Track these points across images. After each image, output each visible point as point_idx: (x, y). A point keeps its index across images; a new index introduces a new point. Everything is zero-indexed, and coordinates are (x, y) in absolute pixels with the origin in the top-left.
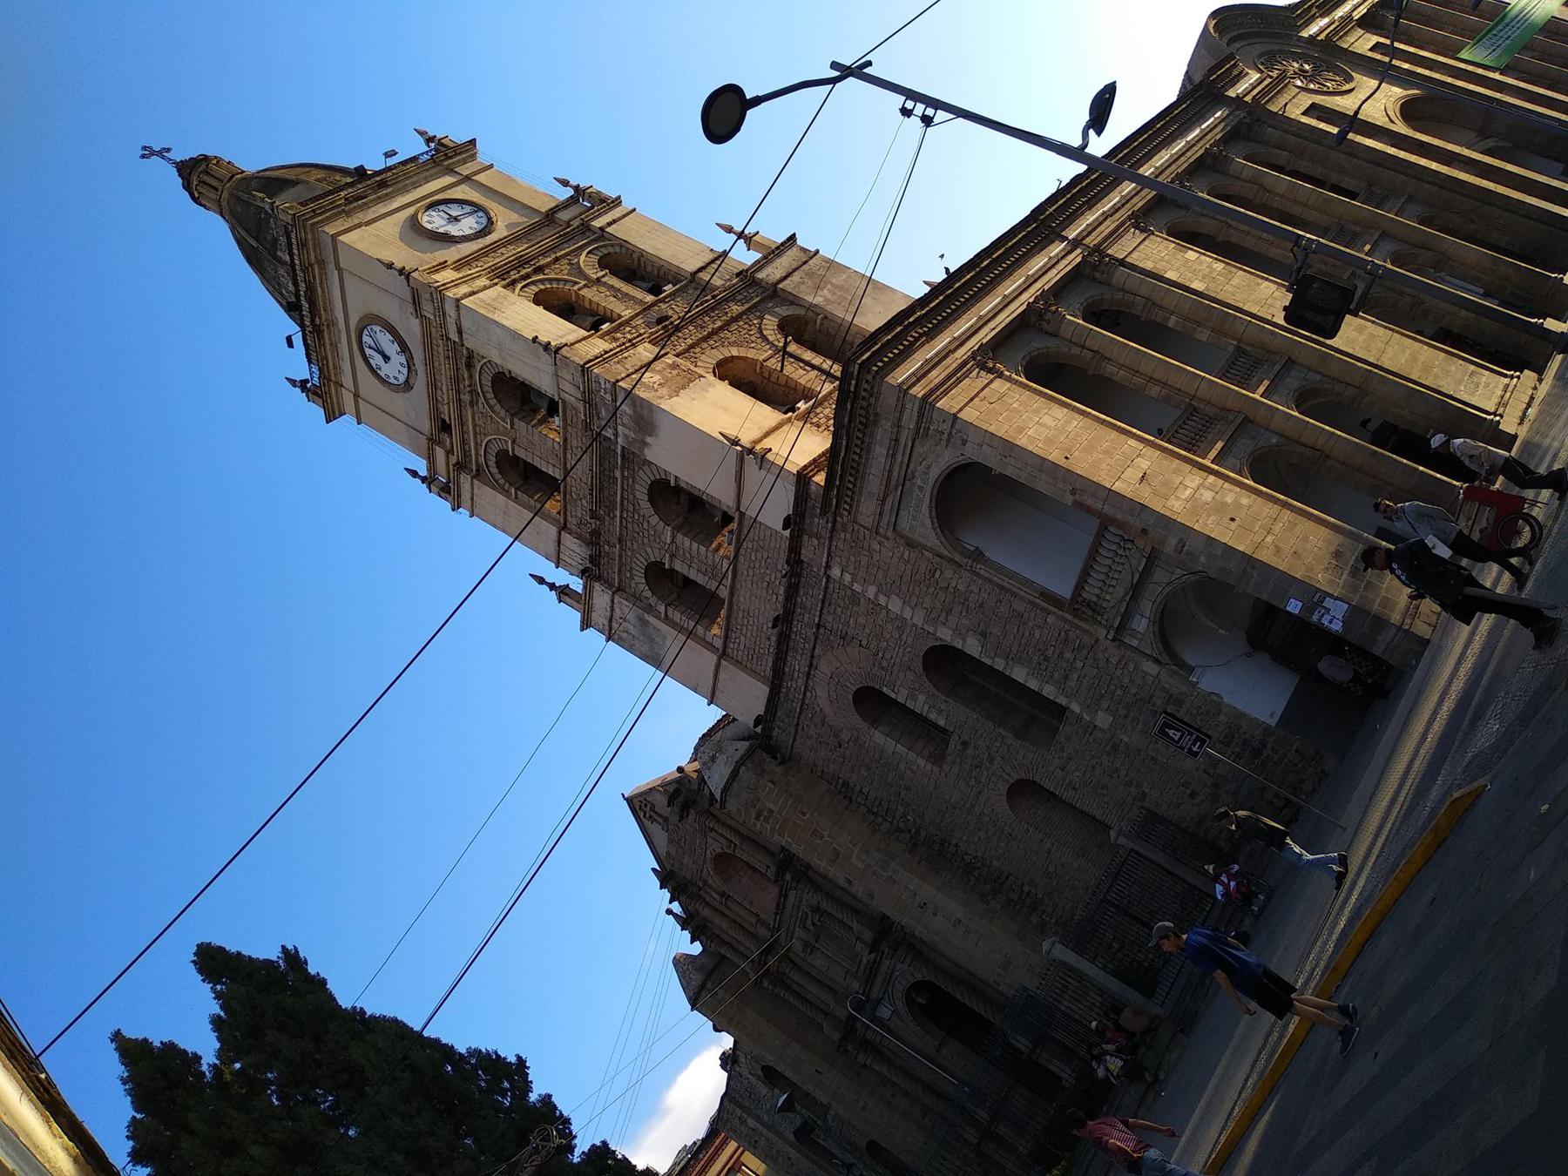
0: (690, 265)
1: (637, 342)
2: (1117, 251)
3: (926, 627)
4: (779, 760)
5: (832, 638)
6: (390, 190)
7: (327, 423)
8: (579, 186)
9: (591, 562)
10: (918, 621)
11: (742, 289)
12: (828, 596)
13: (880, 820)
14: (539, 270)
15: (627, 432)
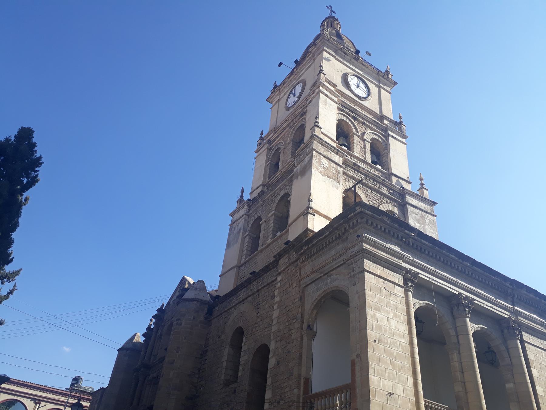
0: (394, 171)
1: (339, 154)
2: (526, 337)
3: (272, 335)
4: (205, 316)
5: (256, 300)
6: (356, 62)
7: (266, 100)
8: (402, 122)
9: (253, 199)
10: (274, 329)
11: (395, 191)
12: (270, 285)
13: (197, 376)
14: (355, 119)
15: (299, 168)
